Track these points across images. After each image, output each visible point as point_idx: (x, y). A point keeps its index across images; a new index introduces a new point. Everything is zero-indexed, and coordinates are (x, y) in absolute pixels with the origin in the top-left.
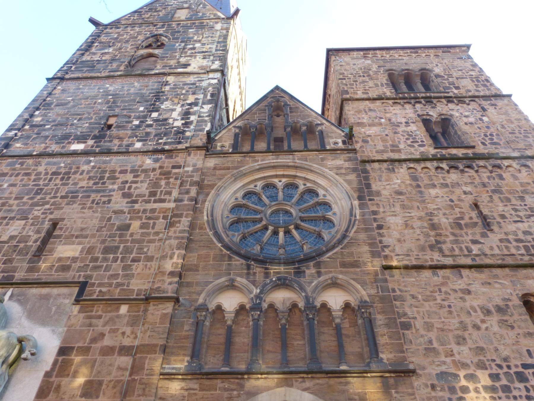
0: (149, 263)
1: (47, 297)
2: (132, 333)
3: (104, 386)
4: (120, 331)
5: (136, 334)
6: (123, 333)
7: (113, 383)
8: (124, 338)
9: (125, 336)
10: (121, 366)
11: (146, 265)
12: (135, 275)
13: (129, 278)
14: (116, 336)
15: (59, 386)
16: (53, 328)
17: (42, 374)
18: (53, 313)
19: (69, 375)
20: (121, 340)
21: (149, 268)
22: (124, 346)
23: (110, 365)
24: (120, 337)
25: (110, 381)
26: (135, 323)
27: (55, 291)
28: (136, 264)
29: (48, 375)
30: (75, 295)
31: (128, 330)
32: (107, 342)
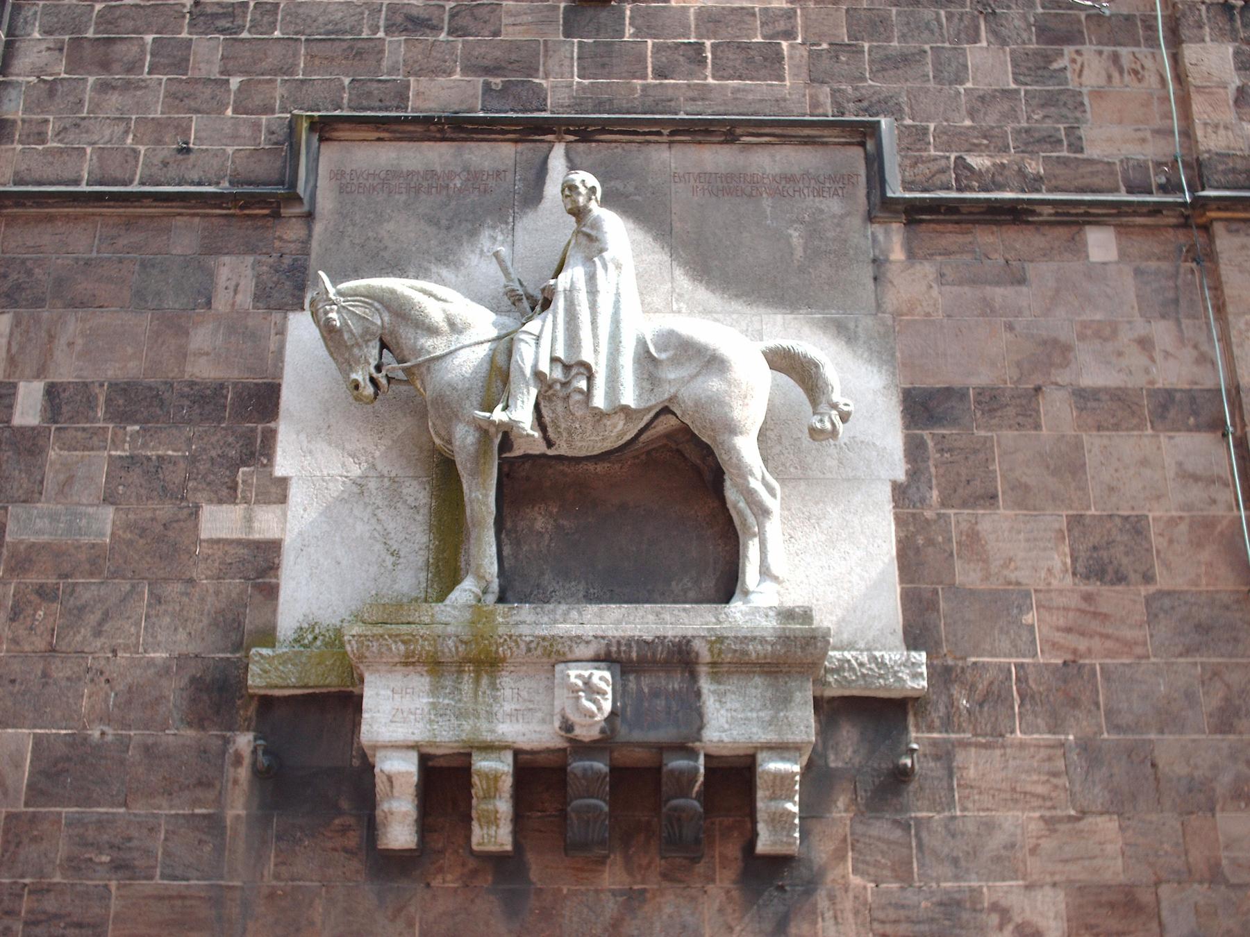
0: (1124, 51)
1: (731, 186)
2: (1181, 340)
3: (1156, 541)
4: (1126, 336)
5: (1195, 347)
6: (1145, 344)
7: (1183, 527)
8: (1152, 360)
9: (1158, 356)
10: (1190, 467)
11: (1115, 58)
12: (1086, 101)
13: (1065, 111)
14: (1120, 354)
16: (834, 314)
18: (799, 252)
19: (994, 497)
20: (1147, 371)
21: (1136, 72)
22: (1169, 394)
23: (1144, 462)
24: (1136, 359)
25: (1173, 522)
26: (1176, 301)
27: (769, 161)
28: (1069, 50)
29: (900, 493)
30: (863, 179)
31: (1162, 332)
32: (1094, 377)
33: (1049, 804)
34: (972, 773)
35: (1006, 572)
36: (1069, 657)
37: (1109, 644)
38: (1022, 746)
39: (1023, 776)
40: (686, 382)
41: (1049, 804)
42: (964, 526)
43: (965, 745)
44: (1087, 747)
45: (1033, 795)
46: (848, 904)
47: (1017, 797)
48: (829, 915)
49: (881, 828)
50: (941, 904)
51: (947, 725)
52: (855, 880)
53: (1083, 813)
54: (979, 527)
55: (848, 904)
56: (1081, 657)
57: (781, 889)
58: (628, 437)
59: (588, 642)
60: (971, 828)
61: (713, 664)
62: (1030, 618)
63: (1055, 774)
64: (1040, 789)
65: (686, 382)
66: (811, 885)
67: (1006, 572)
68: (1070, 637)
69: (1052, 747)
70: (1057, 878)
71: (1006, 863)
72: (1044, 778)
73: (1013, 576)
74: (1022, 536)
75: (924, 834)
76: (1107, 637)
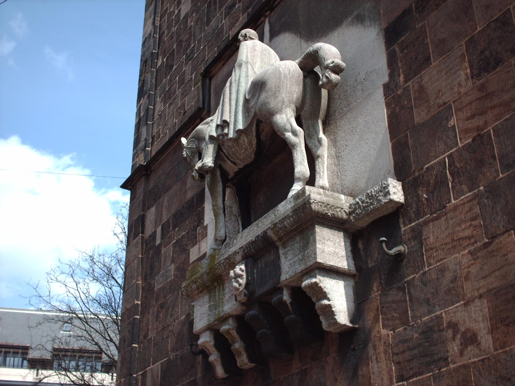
15: (421, 89)
17: (379, 95)
33: (473, 240)
34: (431, 240)
35: (437, 101)
36: (475, 134)
37: (496, 111)
38: (456, 207)
39: (458, 228)
40: (256, 103)
41: (473, 240)
42: (416, 87)
43: (426, 223)
44: (493, 191)
45: (463, 238)
46: (381, 348)
47: (455, 244)
48: (374, 358)
49: (394, 295)
50: (423, 333)
51: (418, 214)
52: (384, 332)
53: (493, 238)
54: (423, 83)
55: (381, 348)
56: (482, 130)
57: (354, 349)
58: (254, 142)
59: (238, 253)
60: (434, 276)
61: (280, 239)
62: (453, 122)
63: (473, 219)
64: (467, 233)
65: (256, 103)
66: (366, 341)
67: (437, 101)
68: (473, 121)
69: (470, 201)
70: (481, 291)
71: (454, 294)
72: (468, 224)
73: (441, 101)
74: (443, 73)
75: (412, 290)
76: (495, 107)
